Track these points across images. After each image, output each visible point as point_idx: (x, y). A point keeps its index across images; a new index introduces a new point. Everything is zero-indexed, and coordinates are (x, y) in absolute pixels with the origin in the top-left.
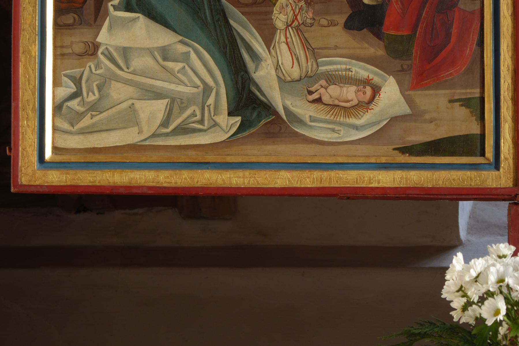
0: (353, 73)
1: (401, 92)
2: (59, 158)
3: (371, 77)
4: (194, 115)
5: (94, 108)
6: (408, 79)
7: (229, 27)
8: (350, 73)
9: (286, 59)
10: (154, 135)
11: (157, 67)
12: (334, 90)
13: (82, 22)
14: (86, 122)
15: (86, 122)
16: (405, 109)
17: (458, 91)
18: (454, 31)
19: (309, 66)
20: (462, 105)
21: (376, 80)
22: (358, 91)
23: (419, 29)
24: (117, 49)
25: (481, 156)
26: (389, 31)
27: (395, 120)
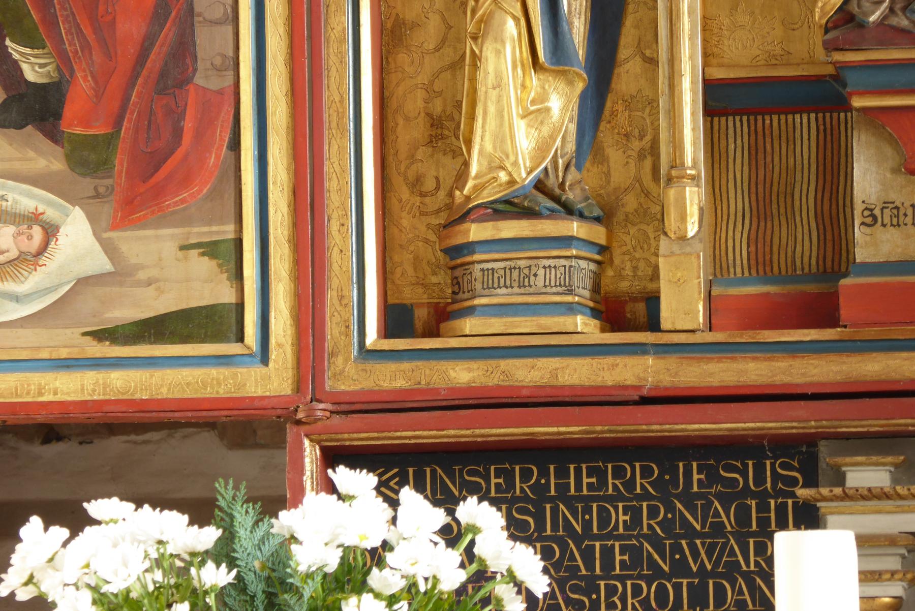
0: (9, 203)
1: (95, 234)
3: (40, 210)
6: (107, 210)
8: (4, 203)
16: (102, 263)
18: (188, 125)
20: (203, 254)
21: (51, 214)
22: (19, 234)
23: (125, 123)
25: (237, 342)
26: (72, 127)
27: (84, 283)
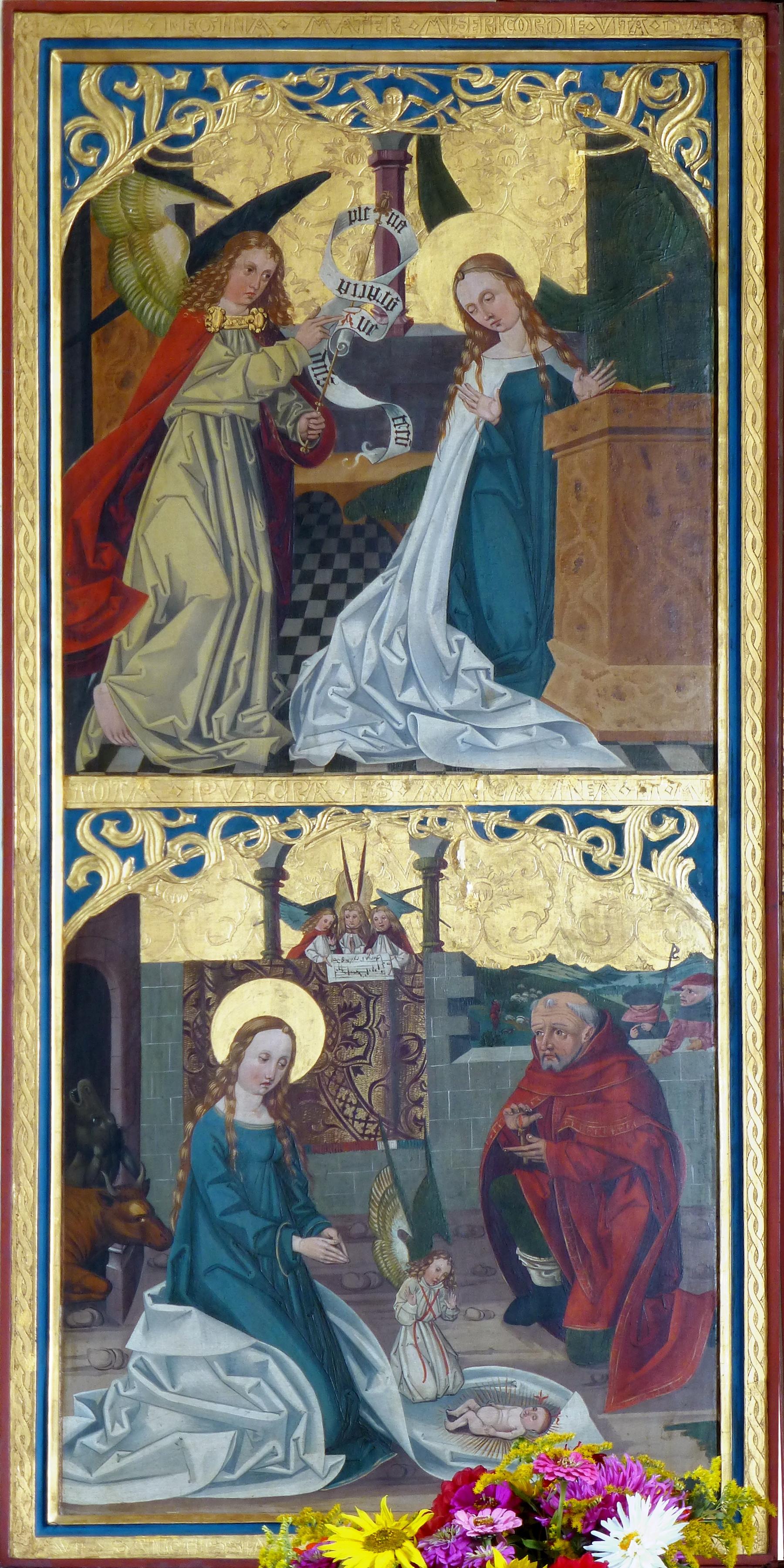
0: (517, 1389)
2: (68, 1520)
3: (544, 1394)
4: (273, 1453)
5: (121, 1445)
7: (328, 1325)
8: (513, 1388)
9: (415, 1370)
10: (213, 1485)
11: (218, 1385)
12: (488, 1414)
13: (105, 1321)
14: (110, 1466)
15: (110, 1466)
17: (679, 1413)
19: (449, 1378)
22: (526, 1415)
23: (619, 1322)
24: (157, 1358)
26: (574, 1325)
